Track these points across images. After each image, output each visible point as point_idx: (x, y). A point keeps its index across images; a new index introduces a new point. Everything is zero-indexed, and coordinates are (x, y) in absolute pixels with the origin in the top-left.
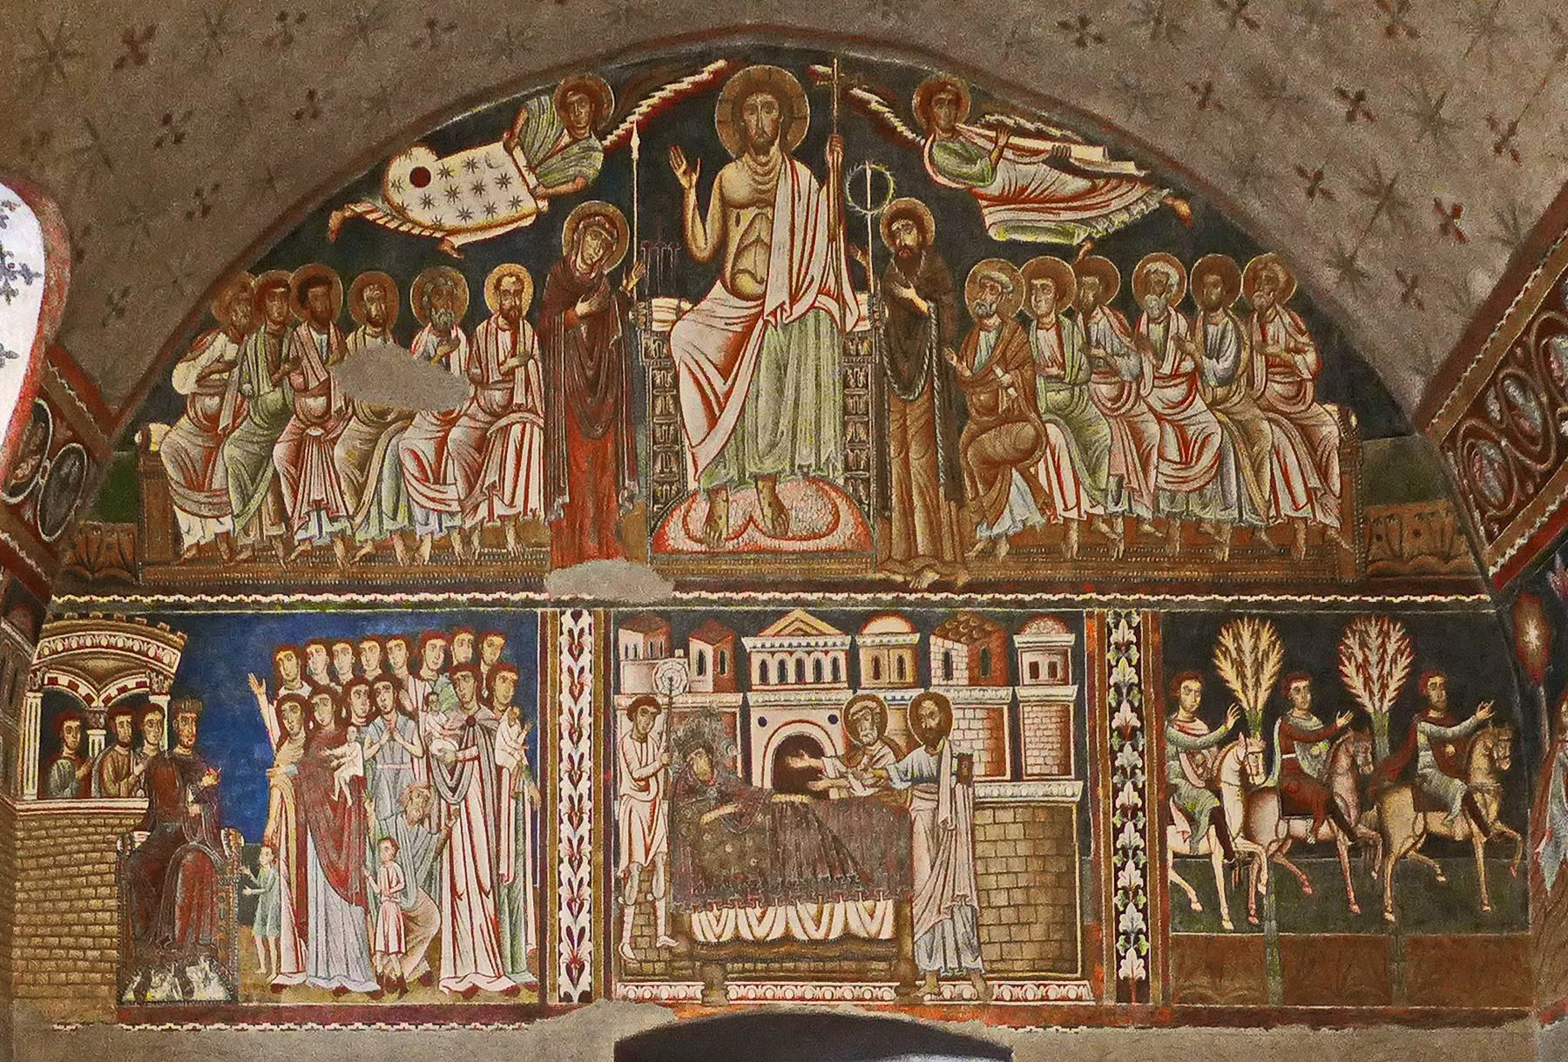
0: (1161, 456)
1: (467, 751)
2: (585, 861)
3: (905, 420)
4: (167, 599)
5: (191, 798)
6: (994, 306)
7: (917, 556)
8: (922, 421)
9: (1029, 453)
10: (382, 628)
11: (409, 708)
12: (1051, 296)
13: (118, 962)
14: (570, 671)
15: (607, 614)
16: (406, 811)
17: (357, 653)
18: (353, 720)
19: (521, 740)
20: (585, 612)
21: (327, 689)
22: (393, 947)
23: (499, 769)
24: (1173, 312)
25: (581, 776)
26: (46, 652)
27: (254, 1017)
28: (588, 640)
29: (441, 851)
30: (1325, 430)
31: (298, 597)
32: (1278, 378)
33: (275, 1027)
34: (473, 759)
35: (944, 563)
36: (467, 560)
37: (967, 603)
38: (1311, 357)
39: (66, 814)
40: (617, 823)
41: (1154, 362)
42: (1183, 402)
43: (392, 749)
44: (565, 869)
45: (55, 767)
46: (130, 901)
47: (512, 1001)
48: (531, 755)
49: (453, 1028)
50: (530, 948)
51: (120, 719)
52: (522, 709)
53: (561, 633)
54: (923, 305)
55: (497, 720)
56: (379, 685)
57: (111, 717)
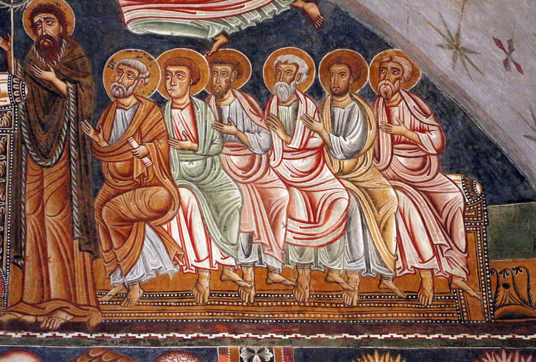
0: (289, 216)
3: (42, 183)
6: (131, 89)
7: (49, 300)
8: (58, 184)
9: (163, 212)
12: (186, 80)
24: (302, 97)
30: (451, 196)
32: (403, 153)
35: (78, 306)
37: (99, 341)
38: (435, 136)
41: (283, 136)
42: (311, 172)
54: (62, 85)
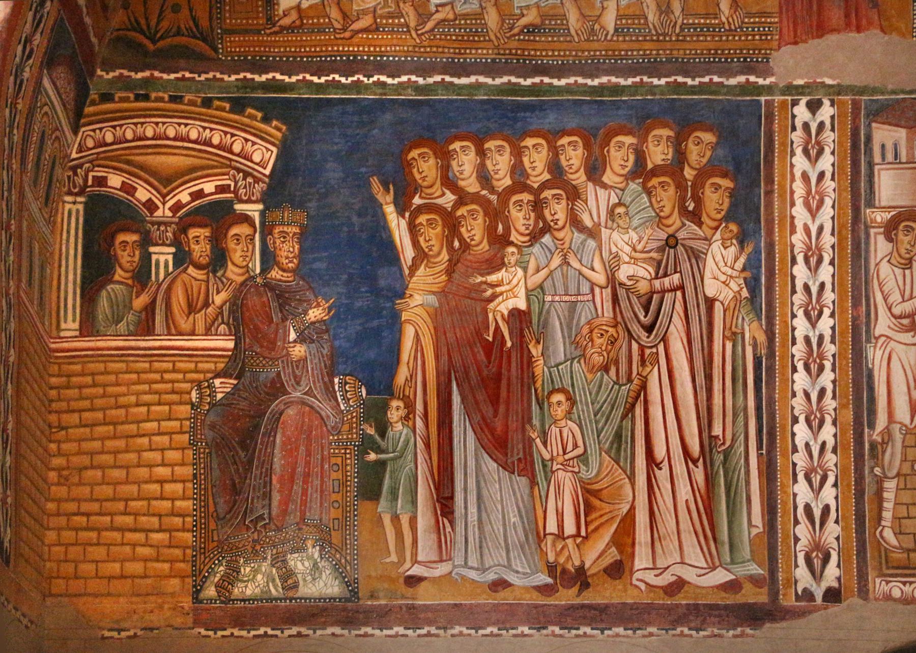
1: (666, 280)
2: (828, 420)
4: (257, 78)
5: (293, 336)
10: (550, 120)
11: (588, 223)
13: (193, 548)
14: (805, 177)
15: (856, 105)
16: (584, 355)
17: (518, 153)
18: (512, 238)
19: (739, 265)
20: (826, 102)
21: (476, 198)
22: (570, 528)
23: (710, 302)
25: (821, 313)
26: (90, 143)
27: (382, 617)
28: (829, 137)
29: (633, 406)
31: (438, 78)
33: (410, 632)
34: (674, 290)
36: (665, 35)
39: (122, 354)
40: (870, 376)
43: (565, 277)
44: (802, 432)
45: (104, 293)
46: (208, 468)
47: (730, 599)
48: (753, 285)
49: (651, 634)
50: (755, 531)
51: (193, 232)
52: (740, 224)
53: (794, 129)
55: (708, 240)
56: (547, 194)
57: (183, 227)
